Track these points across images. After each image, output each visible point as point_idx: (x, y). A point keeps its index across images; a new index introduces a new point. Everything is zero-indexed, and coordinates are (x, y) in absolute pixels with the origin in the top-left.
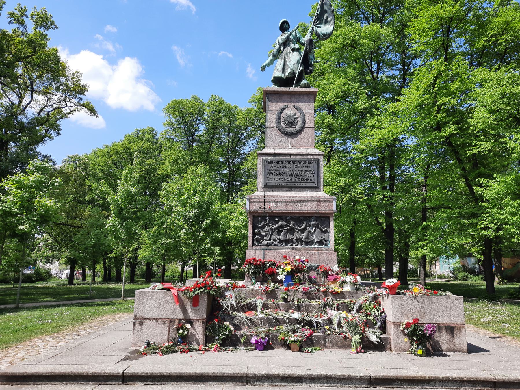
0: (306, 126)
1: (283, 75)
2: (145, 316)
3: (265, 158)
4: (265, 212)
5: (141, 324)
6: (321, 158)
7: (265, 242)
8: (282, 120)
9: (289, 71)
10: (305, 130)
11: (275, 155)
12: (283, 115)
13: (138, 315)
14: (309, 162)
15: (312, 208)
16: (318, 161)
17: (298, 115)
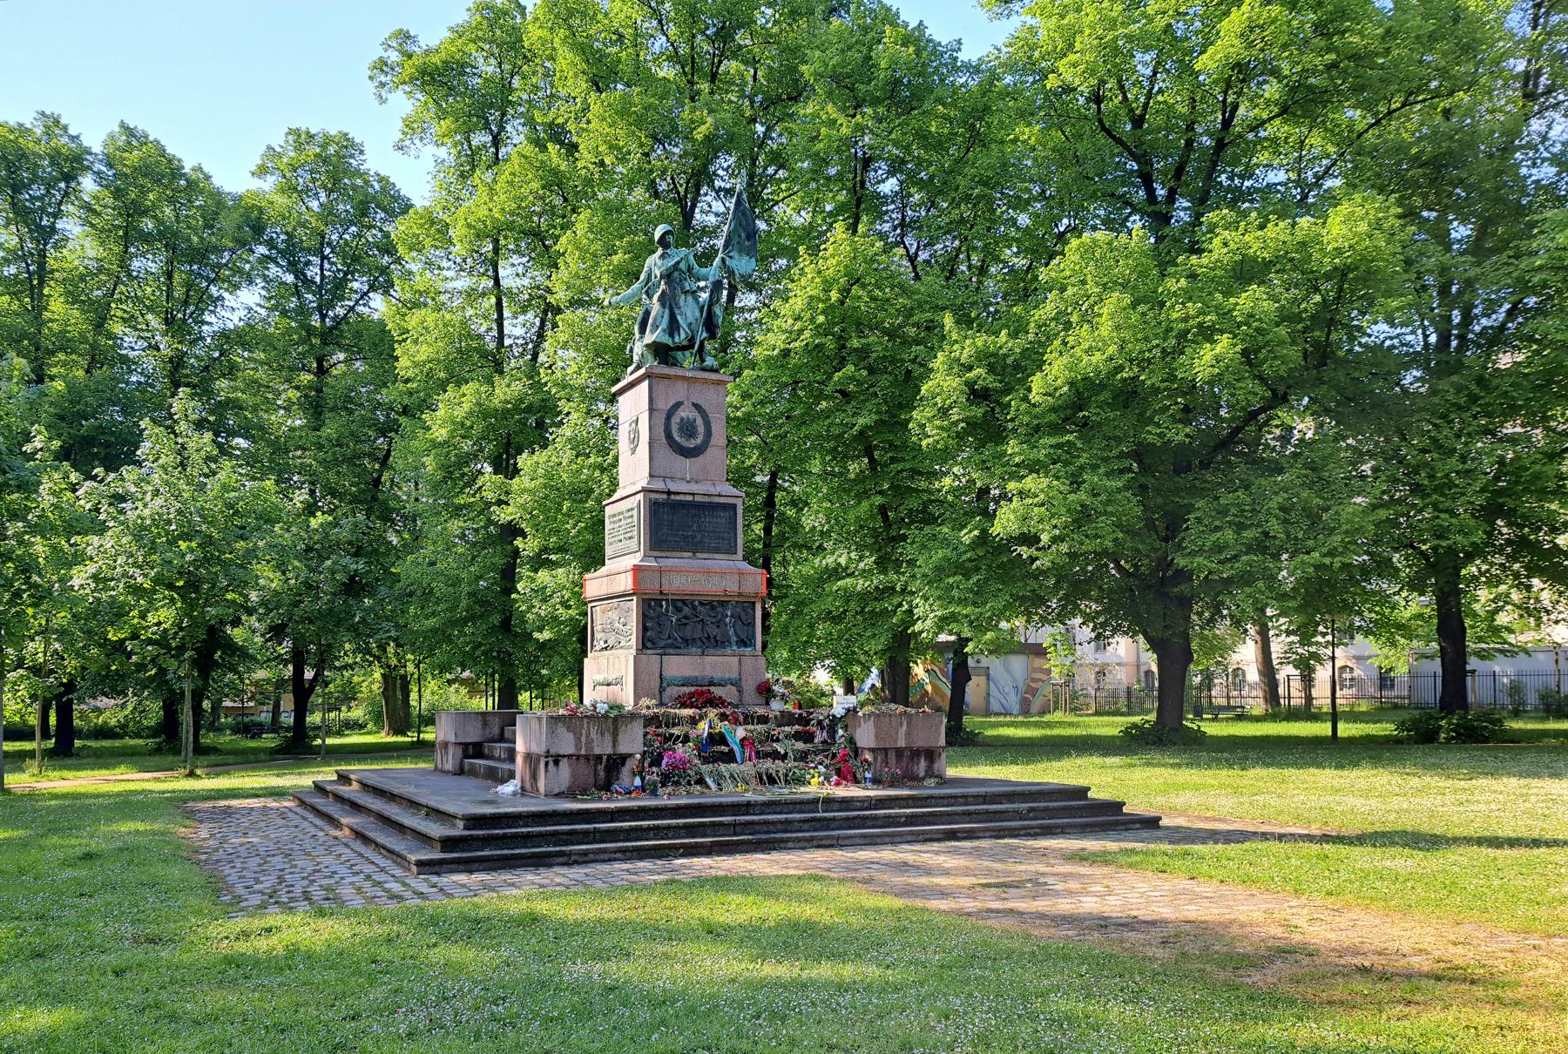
0: (713, 441)
1: (670, 343)
2: (562, 752)
3: (654, 496)
5: (556, 763)
7: (662, 643)
9: (683, 336)
11: (669, 493)
12: (675, 420)
13: (552, 752)
14: (725, 507)
15: (731, 586)
16: (734, 507)
17: (699, 421)
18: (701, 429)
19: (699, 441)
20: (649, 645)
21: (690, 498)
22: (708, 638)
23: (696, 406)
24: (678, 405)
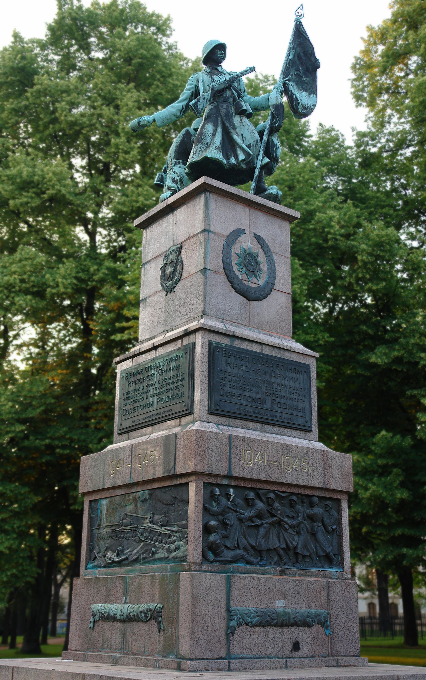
3: (216, 339)
4: (230, 477)
6: (313, 363)
7: (228, 555)
8: (234, 260)
10: (274, 295)
11: (233, 337)
12: (236, 249)
15: (309, 476)
18: (264, 267)
19: (262, 282)
20: (211, 556)
21: (256, 348)
22: (287, 549)
23: (258, 238)
24: (238, 233)
